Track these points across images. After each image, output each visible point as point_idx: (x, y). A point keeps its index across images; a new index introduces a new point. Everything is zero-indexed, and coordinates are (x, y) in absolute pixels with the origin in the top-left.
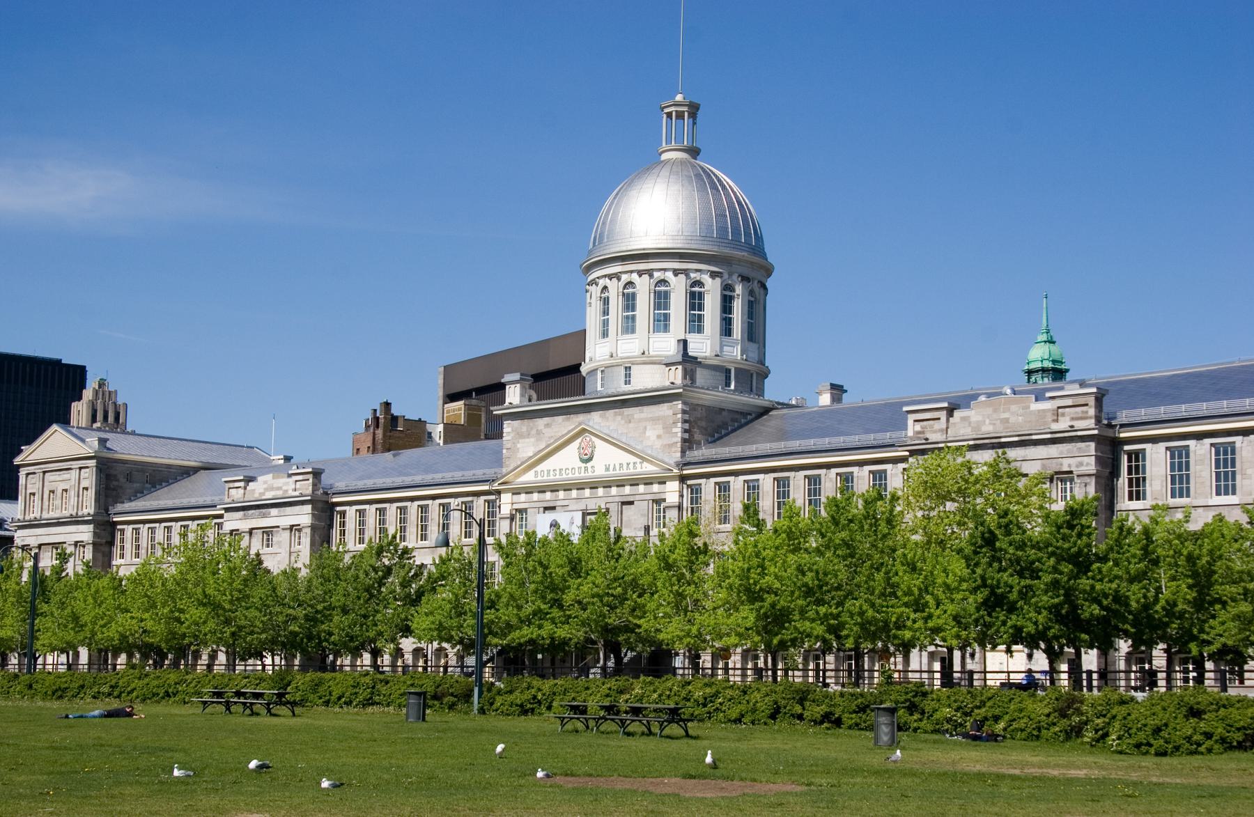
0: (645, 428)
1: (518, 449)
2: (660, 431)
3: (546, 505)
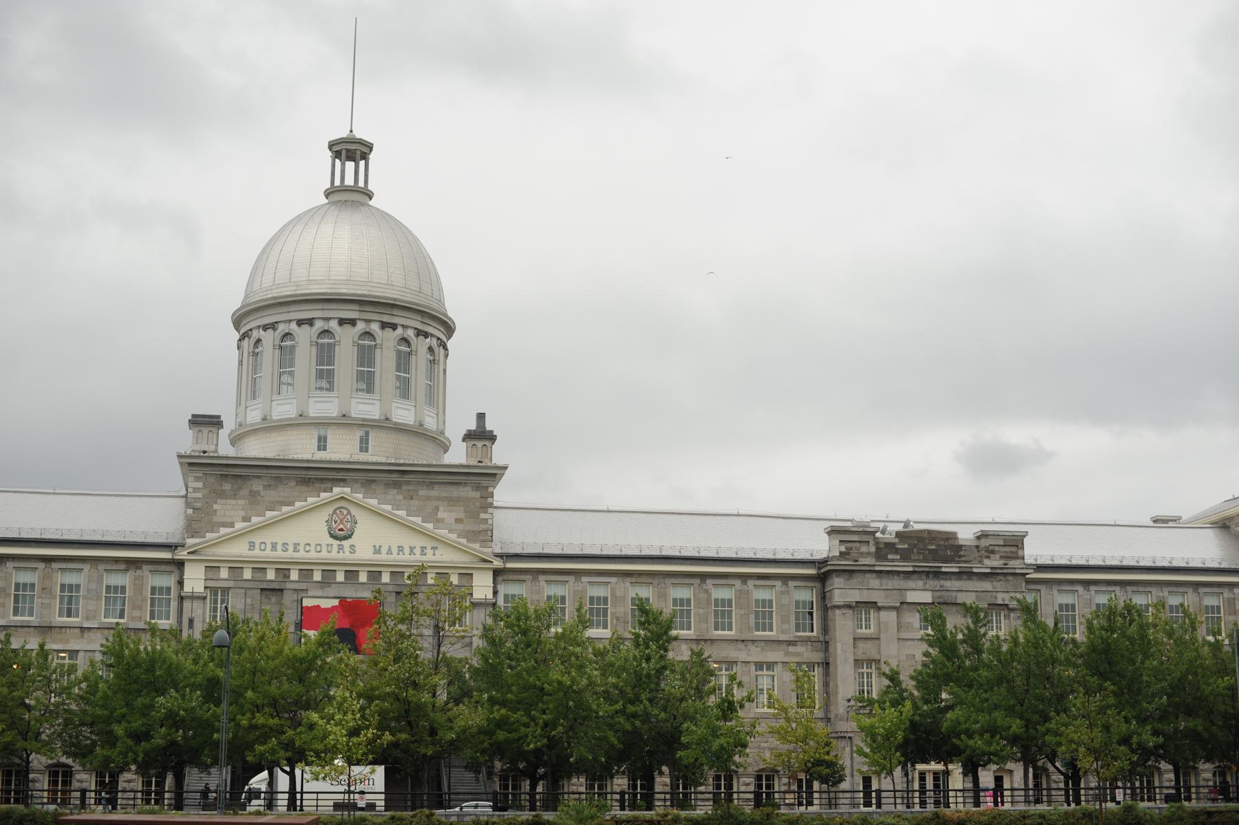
0: (437, 509)
1: (216, 511)
2: (462, 515)
3: (265, 586)
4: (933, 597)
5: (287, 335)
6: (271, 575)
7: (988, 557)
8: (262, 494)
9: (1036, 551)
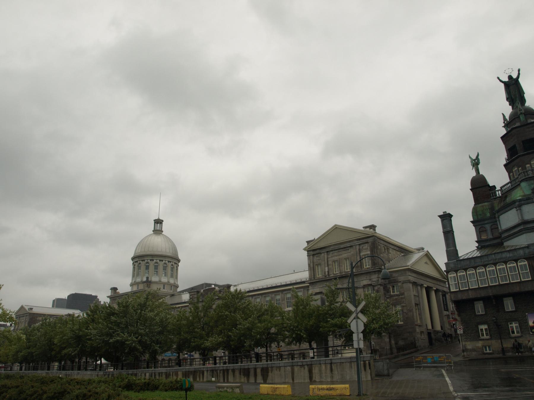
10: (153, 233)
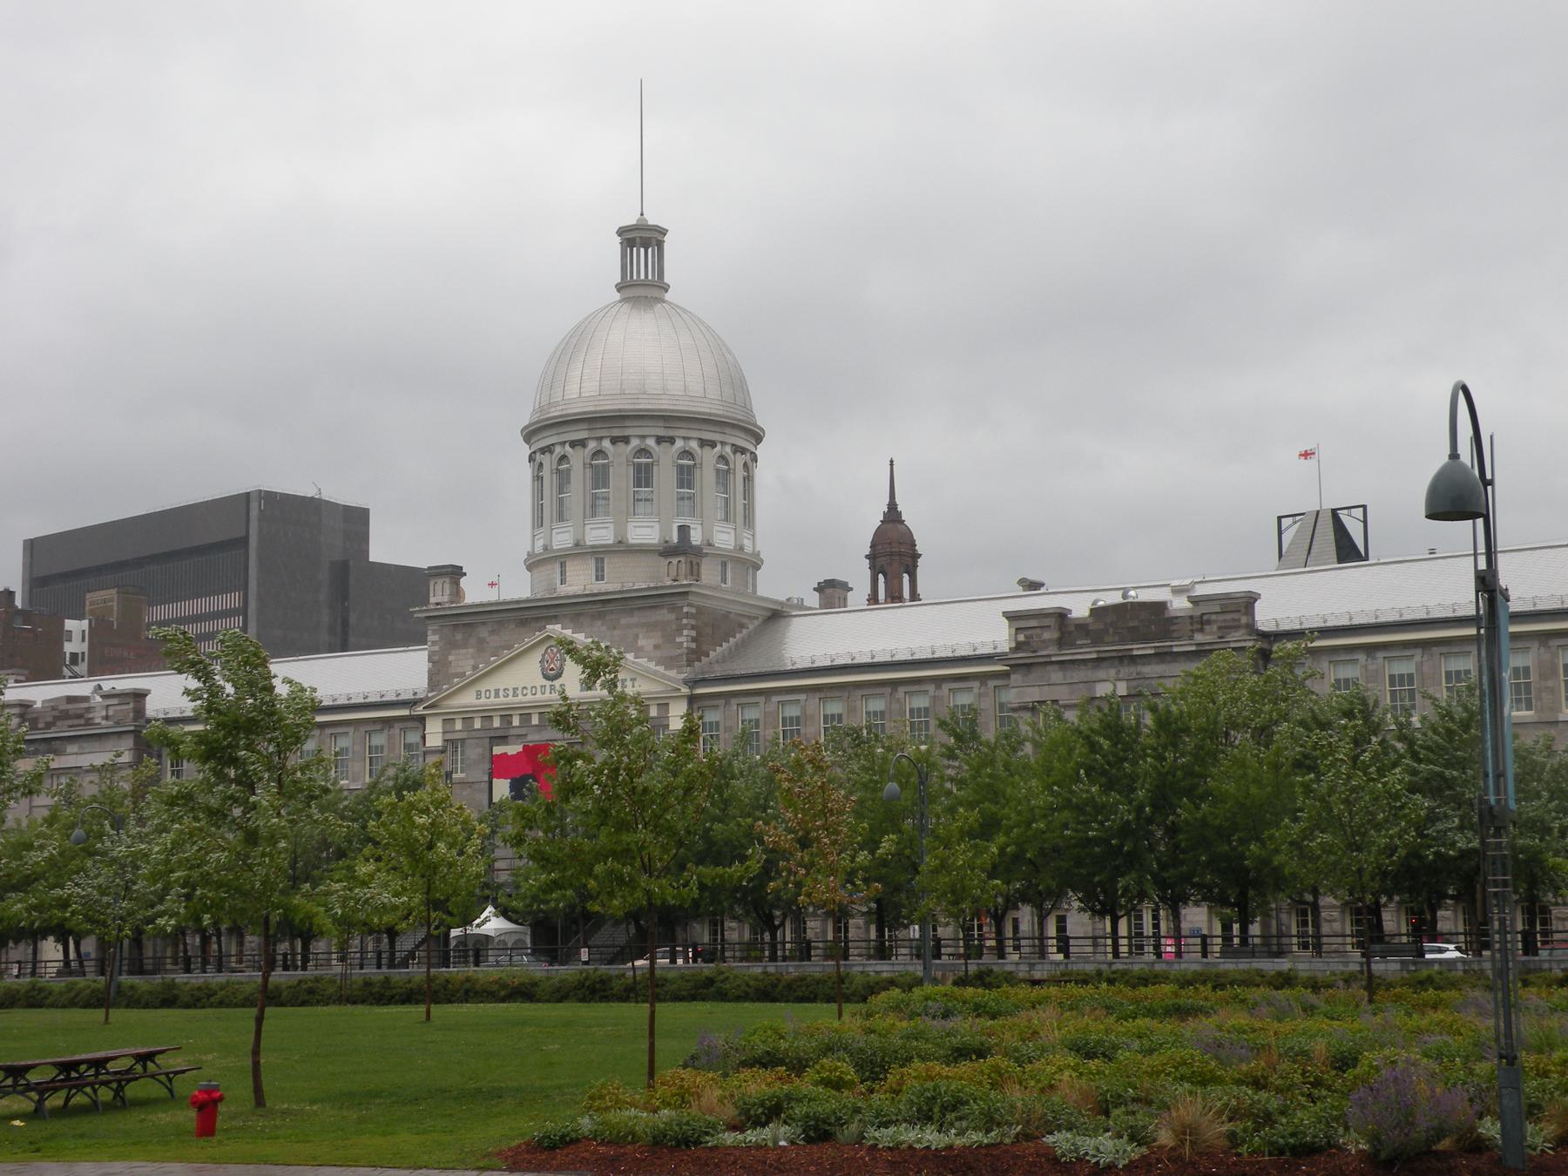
1: (450, 662)
4: (1128, 688)
5: (563, 458)
6: (497, 723)
7: (1201, 630)
8: (488, 640)
9: (1266, 616)
10: (617, 296)
